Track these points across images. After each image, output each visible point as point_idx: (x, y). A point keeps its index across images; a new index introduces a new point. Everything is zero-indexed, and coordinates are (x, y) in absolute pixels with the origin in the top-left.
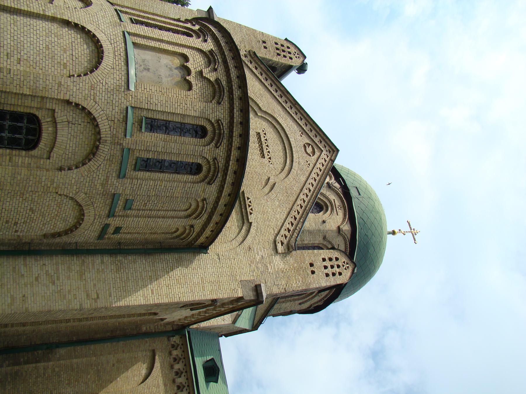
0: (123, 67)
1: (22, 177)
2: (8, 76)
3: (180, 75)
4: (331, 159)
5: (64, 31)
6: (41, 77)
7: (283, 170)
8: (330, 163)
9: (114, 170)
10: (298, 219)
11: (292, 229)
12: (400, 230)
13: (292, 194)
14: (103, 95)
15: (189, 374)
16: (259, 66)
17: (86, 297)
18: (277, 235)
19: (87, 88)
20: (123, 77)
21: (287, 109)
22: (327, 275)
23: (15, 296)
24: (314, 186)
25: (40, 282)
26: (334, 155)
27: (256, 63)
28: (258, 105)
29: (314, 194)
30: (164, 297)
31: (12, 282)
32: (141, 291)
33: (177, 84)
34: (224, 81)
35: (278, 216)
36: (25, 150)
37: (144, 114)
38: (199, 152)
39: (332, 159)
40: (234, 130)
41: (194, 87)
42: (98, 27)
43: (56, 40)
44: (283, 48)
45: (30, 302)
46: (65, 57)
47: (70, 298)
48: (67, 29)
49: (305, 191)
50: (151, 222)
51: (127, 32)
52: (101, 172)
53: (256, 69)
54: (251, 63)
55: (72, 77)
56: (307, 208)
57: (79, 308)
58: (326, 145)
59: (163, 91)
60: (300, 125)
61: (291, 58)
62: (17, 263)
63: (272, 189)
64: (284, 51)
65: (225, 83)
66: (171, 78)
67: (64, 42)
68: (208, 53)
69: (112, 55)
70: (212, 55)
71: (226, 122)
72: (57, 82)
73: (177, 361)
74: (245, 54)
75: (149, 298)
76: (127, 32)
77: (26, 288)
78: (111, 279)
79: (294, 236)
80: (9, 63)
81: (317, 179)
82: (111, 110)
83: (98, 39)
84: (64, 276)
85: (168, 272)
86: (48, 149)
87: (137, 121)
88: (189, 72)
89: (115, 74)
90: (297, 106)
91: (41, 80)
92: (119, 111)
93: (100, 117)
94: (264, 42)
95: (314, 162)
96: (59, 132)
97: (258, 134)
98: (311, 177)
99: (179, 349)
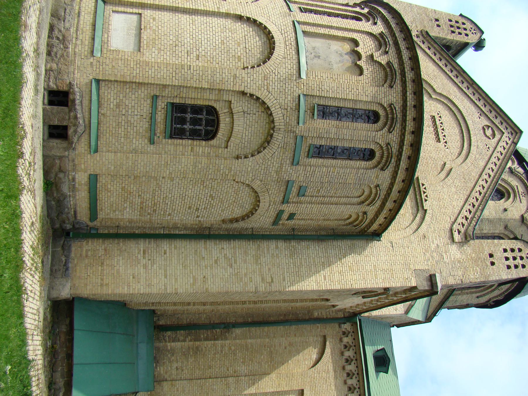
0: (294, 56)
1: (203, 165)
2: (189, 72)
3: (350, 60)
4: (513, 142)
5: (237, 25)
6: (218, 71)
7: (460, 154)
8: (512, 146)
9: (288, 158)
10: (476, 206)
11: (469, 217)
13: (470, 180)
14: (276, 85)
15: (359, 361)
16: (432, 45)
17: (261, 280)
18: (454, 223)
19: (260, 78)
20: (294, 66)
21: (464, 89)
22: (509, 267)
23: (197, 277)
24: (494, 171)
25: (219, 264)
26: (517, 137)
27: (429, 43)
28: (432, 87)
29: (495, 180)
30: (337, 283)
31: (194, 264)
32: (314, 277)
33: (348, 69)
34: (396, 64)
35: (454, 203)
36: (205, 140)
37: (316, 101)
38: (371, 137)
39: (515, 141)
40: (408, 114)
41: (365, 72)
43: (230, 35)
44: (458, 25)
45: (209, 283)
46: (239, 50)
47: (246, 281)
48: (240, 24)
49: (485, 177)
50: (325, 209)
51: (297, 21)
52: (275, 160)
53: (429, 49)
54: (424, 43)
55: (246, 69)
57: (254, 291)
58: (507, 126)
59: (334, 78)
60: (478, 106)
61: (467, 35)
62: (198, 246)
63: (448, 174)
64: (458, 28)
65: (396, 66)
66: (342, 64)
67: (238, 36)
68: (378, 36)
69: (283, 45)
70: (382, 37)
71: (399, 106)
72: (232, 75)
73: (347, 349)
74: (417, 35)
75: (321, 284)
76: (297, 21)
77: (206, 270)
78: (285, 264)
79: (472, 225)
80: (189, 60)
81: (498, 163)
82: (284, 98)
83: (269, 30)
84: (240, 260)
85: (340, 259)
86: (225, 139)
87: (309, 108)
88: (359, 57)
89: (287, 64)
90: (474, 86)
91: (218, 74)
92: (292, 99)
93: (273, 106)
94: (437, 20)
96: (235, 123)
97: (433, 117)
98: (490, 161)
99: (350, 335)
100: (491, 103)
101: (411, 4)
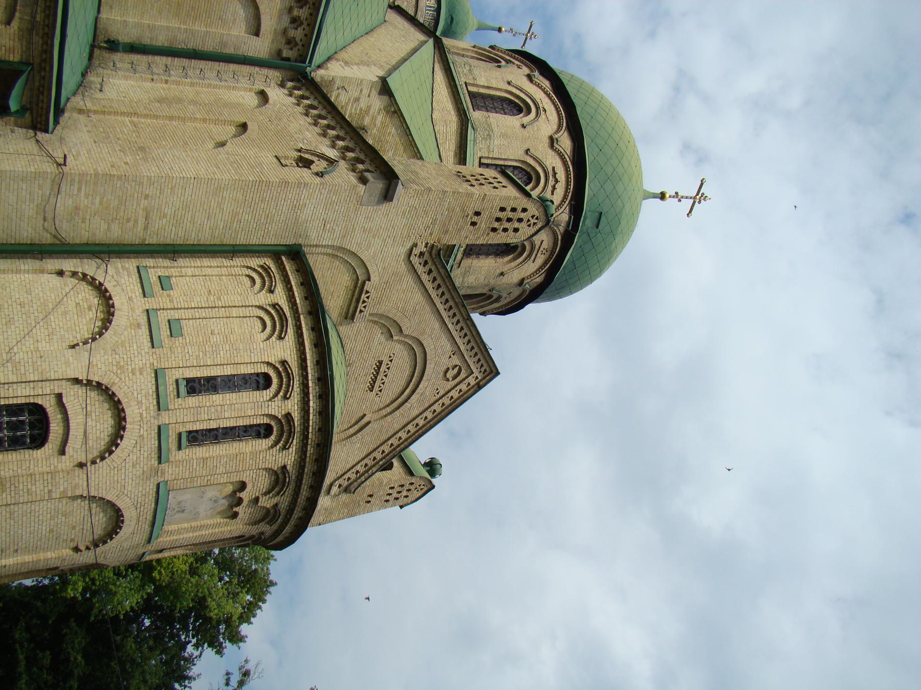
4: (478, 384)
5: (75, 505)
8: (472, 390)
12: (676, 193)
24: (427, 420)
26: (487, 378)
29: (420, 432)
42: (123, 490)
55: (79, 552)
56: (398, 449)
64: (509, 220)
69: (134, 522)
90: (468, 322)
95: (449, 387)
100: (479, 342)
101: (444, 192)
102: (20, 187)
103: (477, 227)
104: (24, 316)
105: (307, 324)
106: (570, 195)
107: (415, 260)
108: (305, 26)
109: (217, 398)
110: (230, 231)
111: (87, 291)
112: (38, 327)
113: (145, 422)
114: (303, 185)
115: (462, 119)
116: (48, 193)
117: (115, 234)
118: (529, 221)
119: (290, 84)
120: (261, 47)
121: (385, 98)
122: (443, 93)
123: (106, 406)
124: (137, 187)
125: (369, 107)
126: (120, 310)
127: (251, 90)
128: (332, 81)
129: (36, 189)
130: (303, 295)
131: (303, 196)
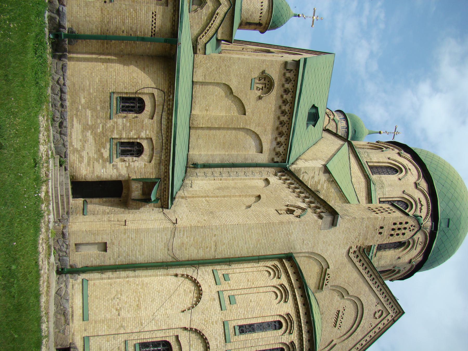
4: (393, 319)
7: (347, 332)
8: (390, 323)
24: (367, 341)
26: (398, 316)
39: (395, 319)
64: (399, 229)
90: (384, 286)
100: (391, 296)
101: (363, 219)
102: (157, 235)
103: (382, 234)
104: (160, 297)
105: (298, 294)
106: (430, 212)
107: (352, 255)
108: (284, 145)
109: (255, 335)
110: (256, 249)
111: (189, 283)
112: (166, 302)
113: (219, 349)
114: (290, 223)
115: (367, 180)
116: (169, 238)
117: (201, 254)
118: (410, 228)
119: (279, 174)
120: (264, 158)
121: (327, 175)
122: (355, 168)
123: (200, 341)
124: (210, 231)
125: (319, 180)
126: (205, 292)
127: (261, 179)
128: (300, 170)
129: (164, 236)
130: (295, 278)
131: (291, 228)
